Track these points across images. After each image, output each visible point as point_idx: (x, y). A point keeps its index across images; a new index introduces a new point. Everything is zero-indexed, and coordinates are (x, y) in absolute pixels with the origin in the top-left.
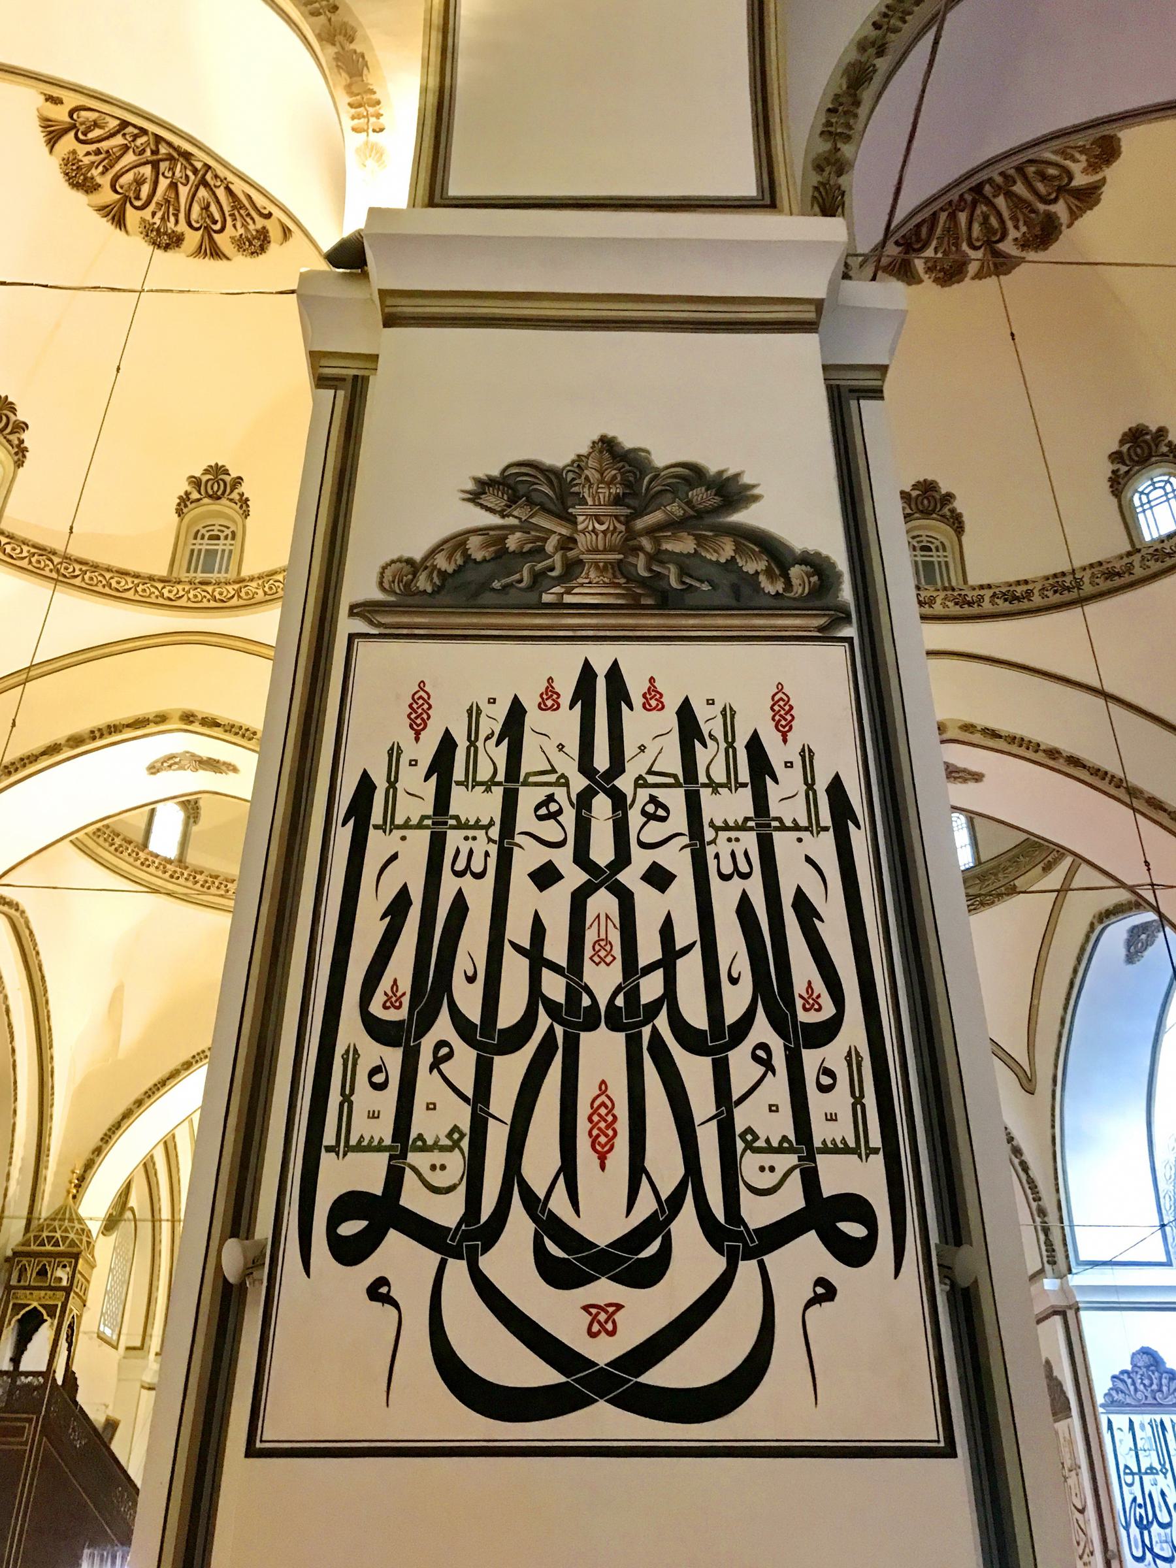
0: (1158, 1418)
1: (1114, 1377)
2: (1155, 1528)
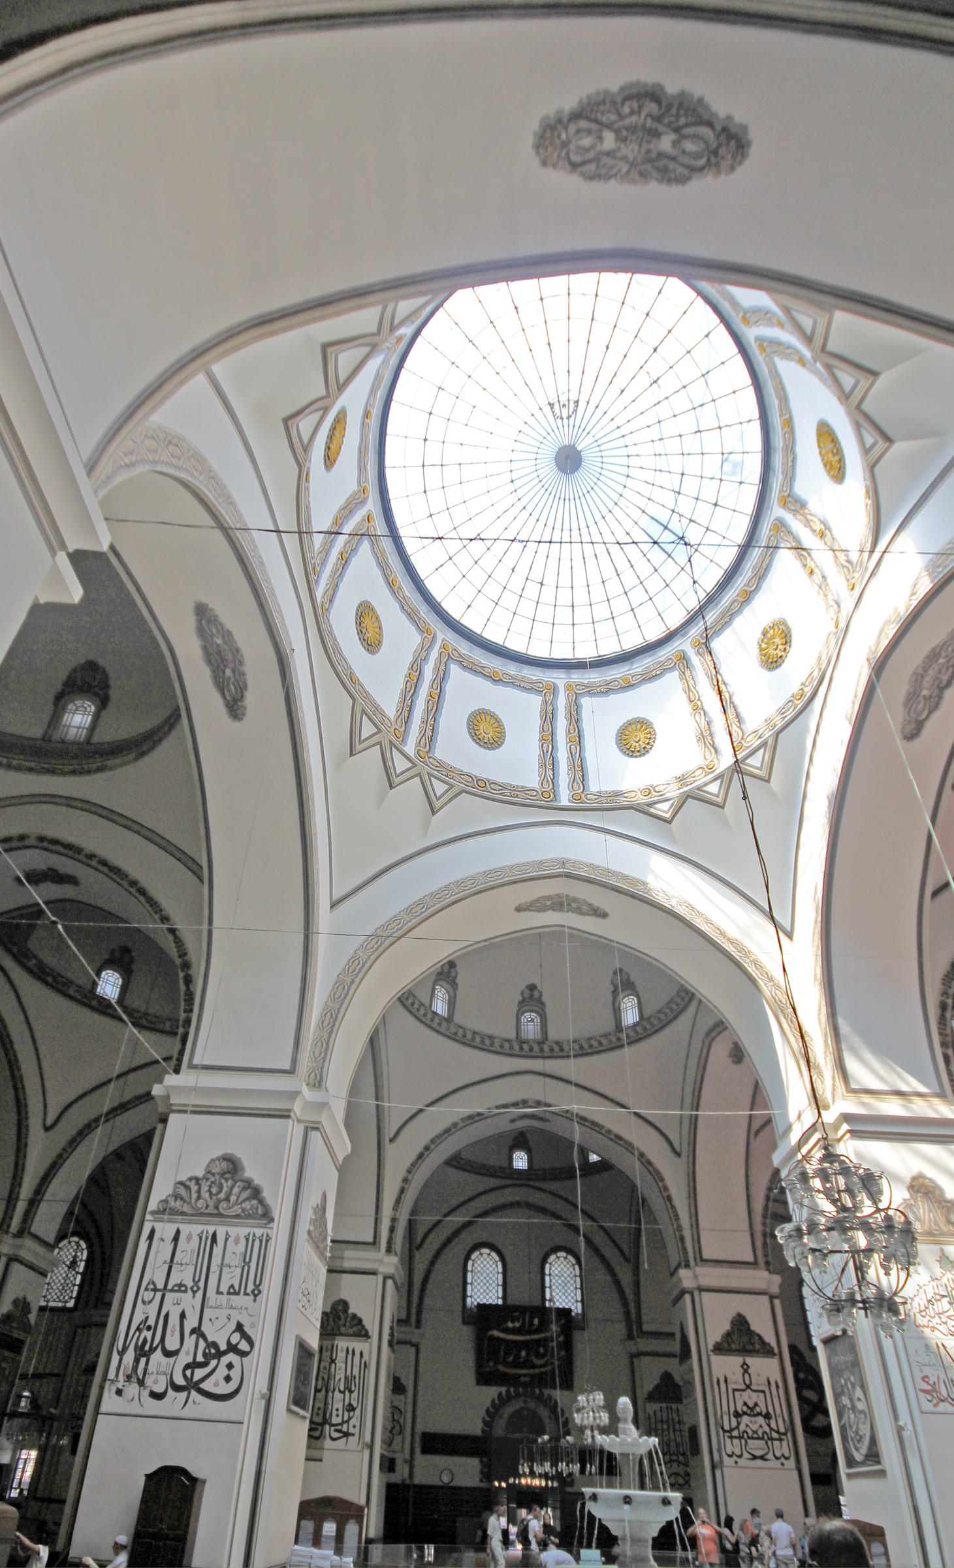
1: (181, 1183)
2: (157, 1356)
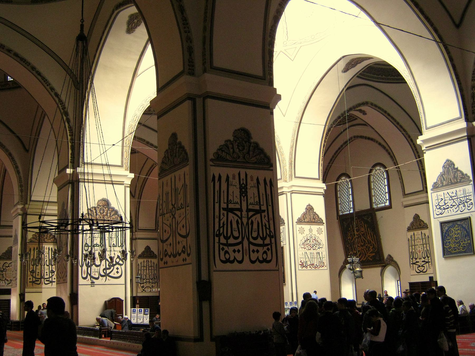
2: (94, 267)
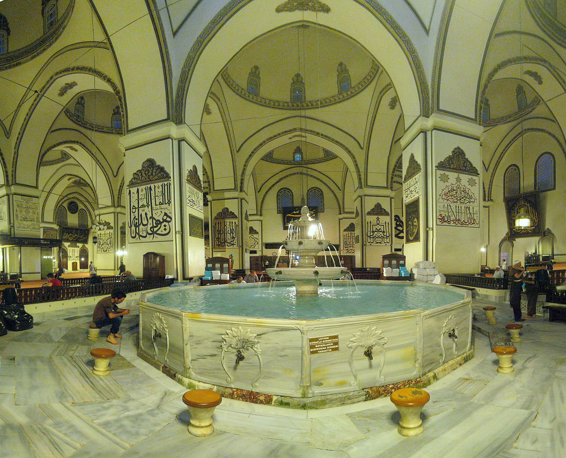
0: (149, 186)
1: (135, 174)
2: (141, 226)
